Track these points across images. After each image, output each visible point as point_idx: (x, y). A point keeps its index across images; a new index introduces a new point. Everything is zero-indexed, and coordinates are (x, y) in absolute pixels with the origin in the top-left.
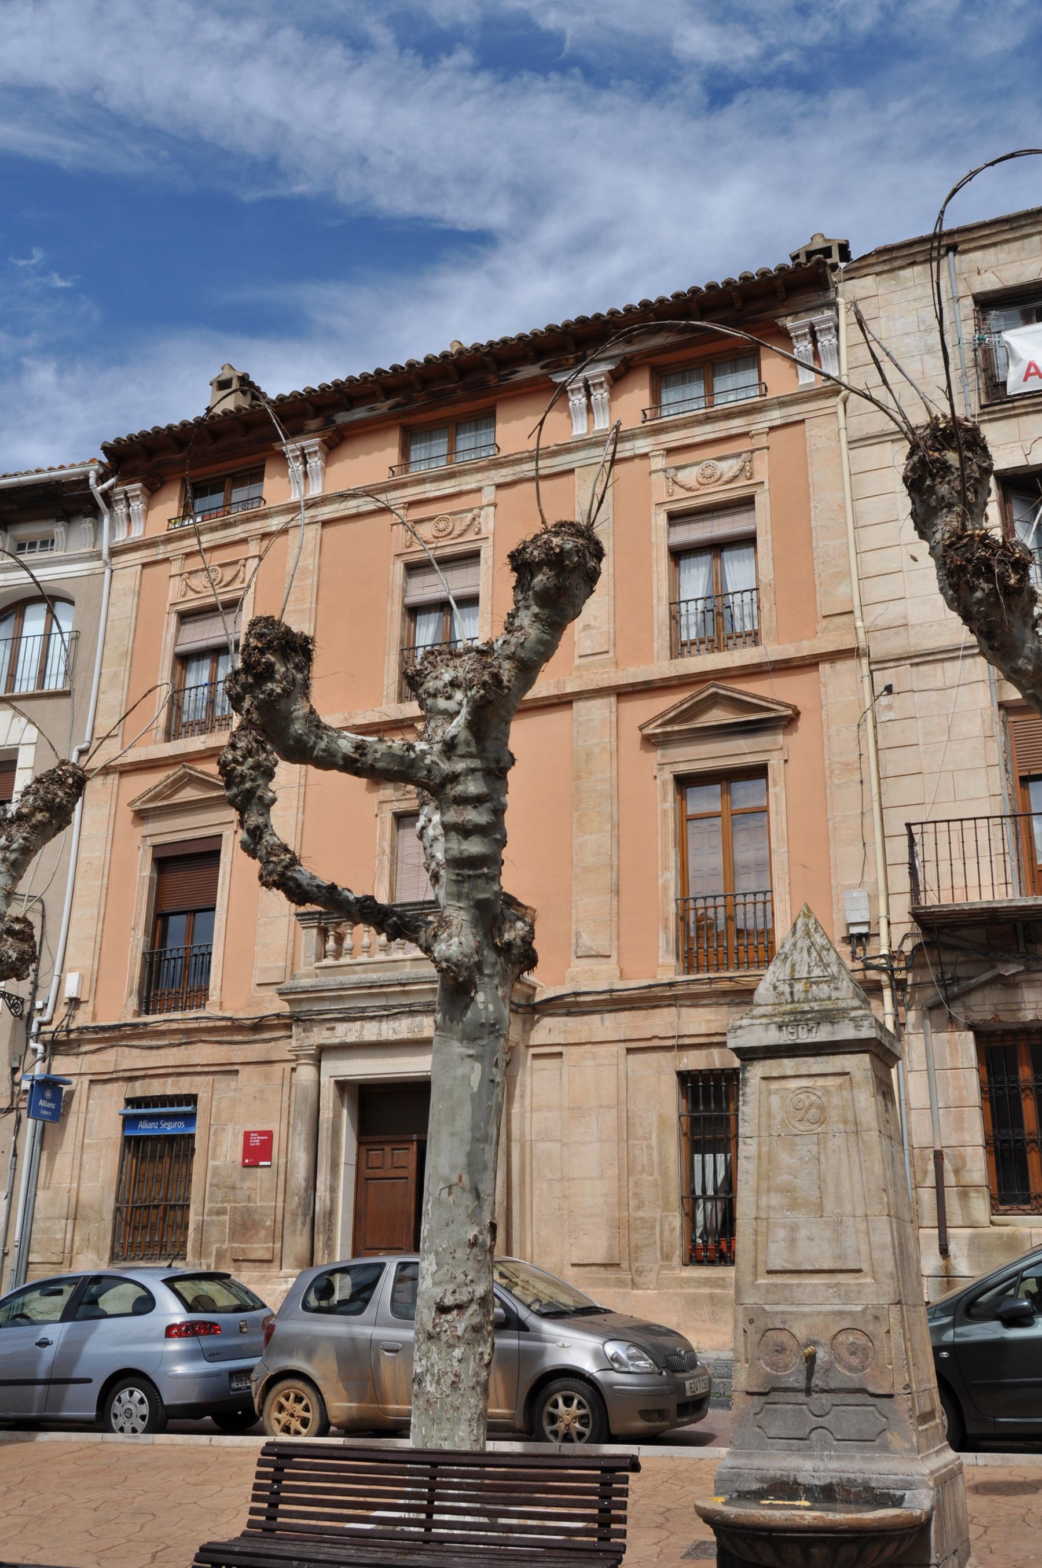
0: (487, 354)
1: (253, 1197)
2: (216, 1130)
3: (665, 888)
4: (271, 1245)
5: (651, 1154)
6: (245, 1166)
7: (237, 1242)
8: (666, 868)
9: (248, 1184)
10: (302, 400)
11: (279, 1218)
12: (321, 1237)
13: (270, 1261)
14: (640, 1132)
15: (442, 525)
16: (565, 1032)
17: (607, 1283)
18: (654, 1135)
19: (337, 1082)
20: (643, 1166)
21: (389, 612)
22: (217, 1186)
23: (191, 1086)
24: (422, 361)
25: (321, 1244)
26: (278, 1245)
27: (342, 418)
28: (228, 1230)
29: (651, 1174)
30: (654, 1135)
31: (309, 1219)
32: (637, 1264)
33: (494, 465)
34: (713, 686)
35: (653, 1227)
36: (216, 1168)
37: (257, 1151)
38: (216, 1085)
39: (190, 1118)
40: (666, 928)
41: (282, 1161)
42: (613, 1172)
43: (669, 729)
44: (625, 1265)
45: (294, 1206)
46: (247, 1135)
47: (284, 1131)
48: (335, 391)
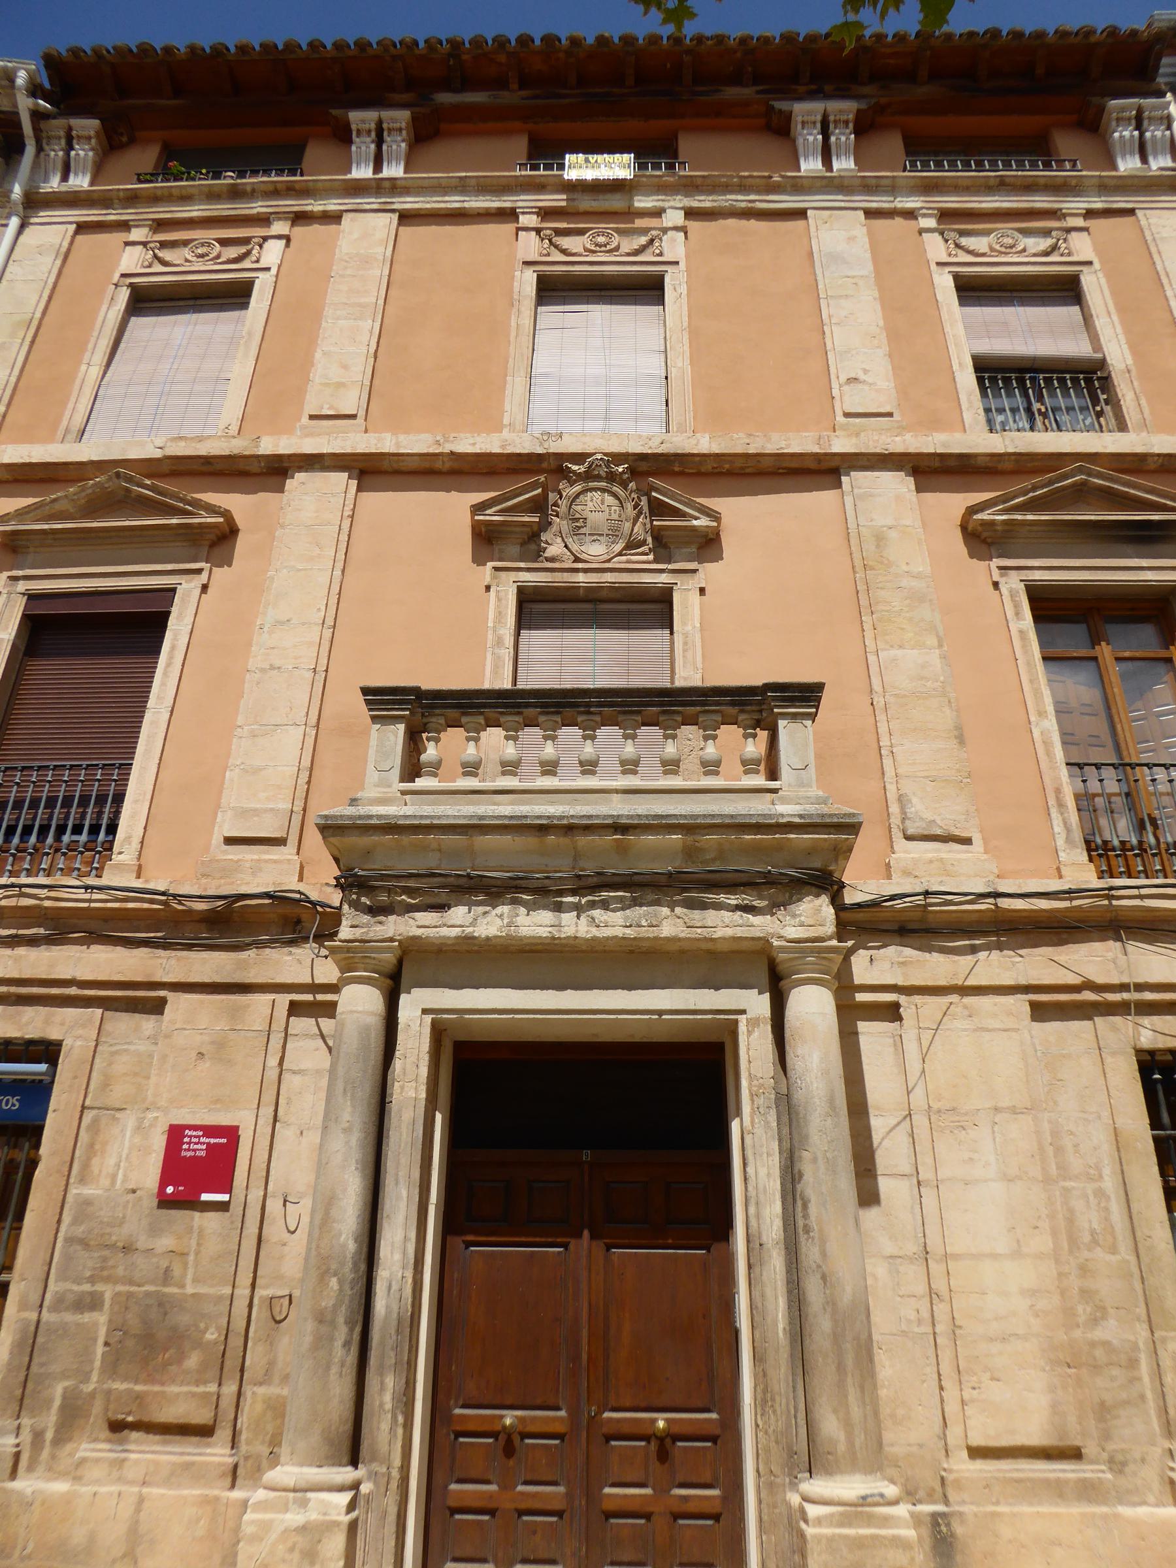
0: (689, 52)
1: (177, 1271)
2: (95, 1121)
3: (1047, 744)
4: (212, 1388)
5: (1107, 1209)
6: (165, 1202)
7: (126, 1379)
8: (1042, 714)
9: (165, 1242)
10: (394, 57)
11: (239, 1324)
12: (390, 1381)
13: (204, 1431)
14: (1076, 1164)
15: (601, 239)
16: (903, 963)
17: (1058, 1490)
18: (1107, 1171)
19: (434, 1024)
20: (1093, 1232)
21: (513, 324)
22: (84, 1243)
23: (47, 1022)
24: (590, 40)
25: (388, 1398)
26: (230, 1389)
27: (445, 98)
28: (100, 1349)
29: (1113, 1250)
30: (1107, 1171)
31: (358, 1329)
32: (1111, 1446)
33: (685, 186)
34: (1080, 470)
35: (1133, 1363)
36: (87, 1202)
37: (198, 1170)
38: (107, 1026)
39: (37, 1093)
40: (1061, 805)
41: (256, 1194)
42: (1042, 1242)
43: (1018, 517)
44: (1090, 1449)
45: (328, 1302)
46: (176, 1134)
47: (265, 1129)
48: (450, 55)
